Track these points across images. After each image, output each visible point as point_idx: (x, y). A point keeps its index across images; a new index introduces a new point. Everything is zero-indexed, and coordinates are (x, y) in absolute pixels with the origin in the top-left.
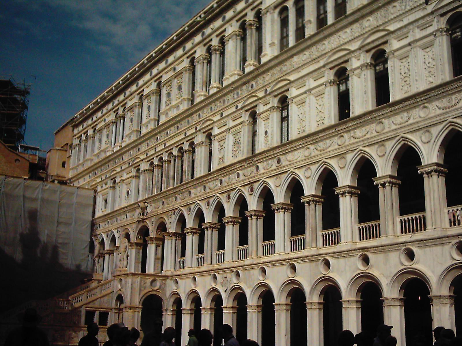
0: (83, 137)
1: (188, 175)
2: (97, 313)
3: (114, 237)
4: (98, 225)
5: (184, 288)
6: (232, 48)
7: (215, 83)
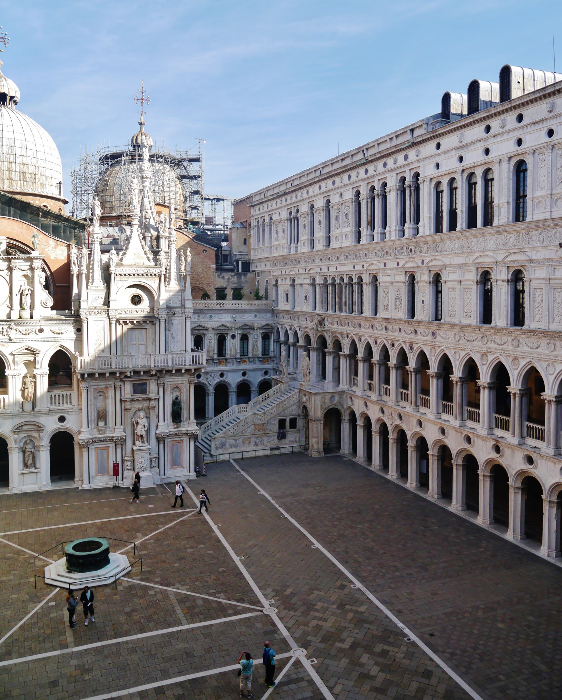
1: (358, 305)
2: (288, 420)
3: (296, 332)
4: (281, 315)
5: (358, 408)
6: (392, 198)
7: (378, 229)
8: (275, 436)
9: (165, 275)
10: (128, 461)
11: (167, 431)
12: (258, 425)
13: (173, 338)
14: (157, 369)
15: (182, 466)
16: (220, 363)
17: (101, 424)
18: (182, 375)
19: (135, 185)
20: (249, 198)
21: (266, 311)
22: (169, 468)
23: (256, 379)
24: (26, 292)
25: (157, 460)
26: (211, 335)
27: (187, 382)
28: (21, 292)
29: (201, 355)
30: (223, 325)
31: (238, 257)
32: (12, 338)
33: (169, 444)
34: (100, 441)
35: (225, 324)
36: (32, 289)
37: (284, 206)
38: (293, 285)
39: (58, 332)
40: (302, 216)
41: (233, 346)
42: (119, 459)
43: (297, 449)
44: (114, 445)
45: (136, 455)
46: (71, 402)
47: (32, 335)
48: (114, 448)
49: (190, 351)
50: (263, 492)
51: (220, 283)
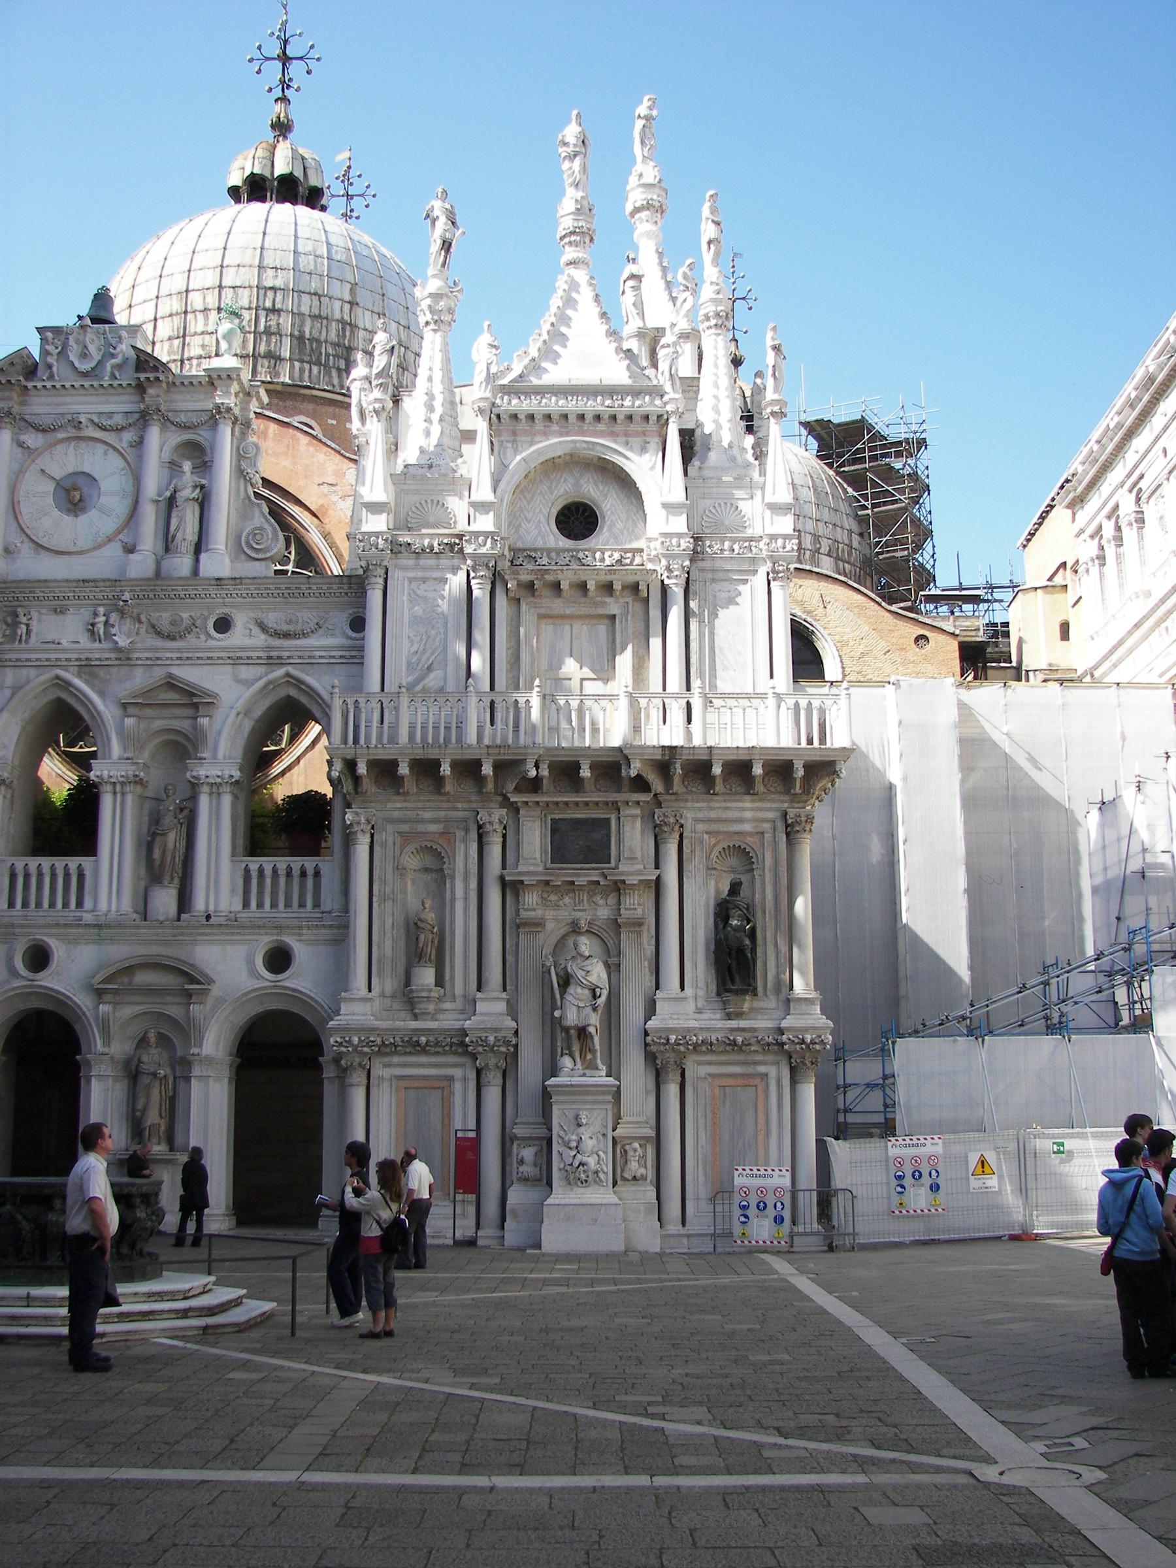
0: (1108, 530)
11: (693, 1024)
17: (426, 976)
24: (188, 493)
27: (780, 826)
28: (168, 494)
36: (204, 482)
39: (285, 628)
46: (316, 905)
47: (192, 640)
48: (472, 1085)
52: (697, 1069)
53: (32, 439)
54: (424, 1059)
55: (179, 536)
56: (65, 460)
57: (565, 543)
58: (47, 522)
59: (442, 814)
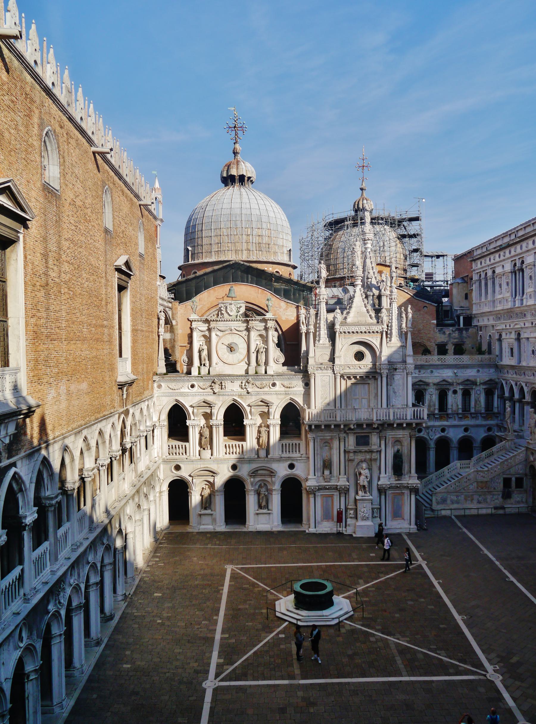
0: (483, 276)
2: (514, 479)
3: (522, 387)
4: (506, 370)
8: (499, 495)
9: (387, 332)
10: (351, 509)
11: (389, 483)
12: (482, 482)
13: (395, 392)
14: (379, 422)
15: (403, 519)
16: (441, 418)
18: (404, 429)
19: (358, 247)
20: (470, 252)
21: (489, 366)
22: (390, 519)
23: (479, 435)
24: (261, 350)
25: (379, 511)
26: (432, 390)
27: (408, 435)
29: (422, 409)
30: (444, 380)
31: (459, 312)
32: (249, 391)
33: (390, 496)
34: (324, 488)
35: (447, 379)
37: (508, 258)
38: (518, 339)
39: (289, 386)
40: (528, 267)
41: (454, 401)
42: (343, 507)
43: (523, 510)
44: (338, 493)
45: (358, 505)
46: (299, 451)
47: (266, 389)
49: (411, 405)
50: (486, 552)
51: (441, 338)
52: (389, 492)
53: (219, 333)
54: (327, 491)
55: (261, 361)
56: (229, 339)
57: (357, 362)
58: (226, 356)
59: (330, 435)
